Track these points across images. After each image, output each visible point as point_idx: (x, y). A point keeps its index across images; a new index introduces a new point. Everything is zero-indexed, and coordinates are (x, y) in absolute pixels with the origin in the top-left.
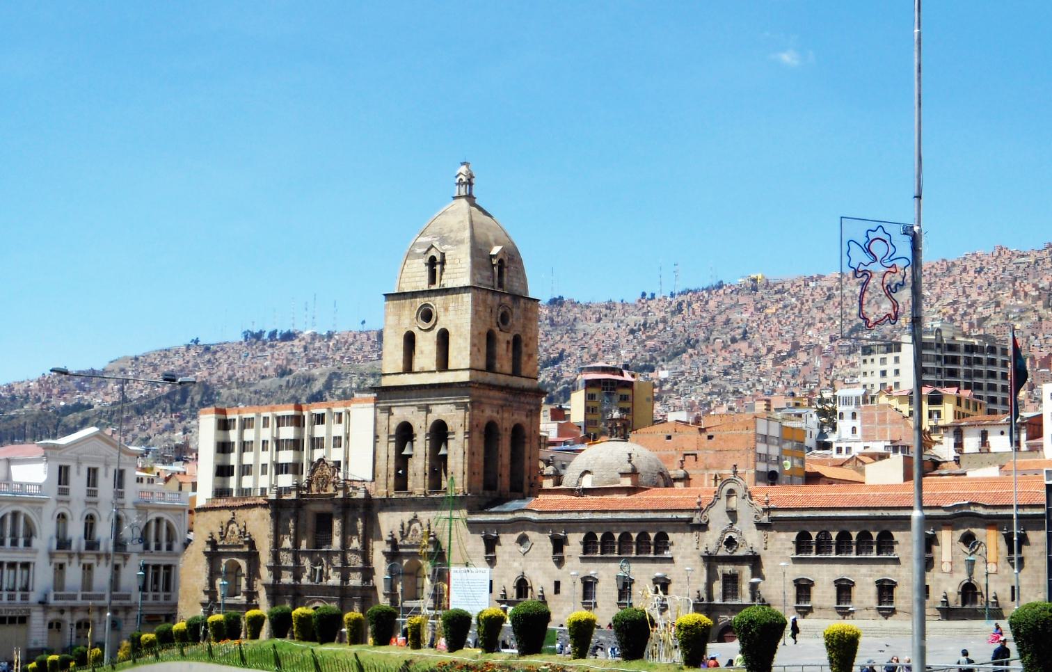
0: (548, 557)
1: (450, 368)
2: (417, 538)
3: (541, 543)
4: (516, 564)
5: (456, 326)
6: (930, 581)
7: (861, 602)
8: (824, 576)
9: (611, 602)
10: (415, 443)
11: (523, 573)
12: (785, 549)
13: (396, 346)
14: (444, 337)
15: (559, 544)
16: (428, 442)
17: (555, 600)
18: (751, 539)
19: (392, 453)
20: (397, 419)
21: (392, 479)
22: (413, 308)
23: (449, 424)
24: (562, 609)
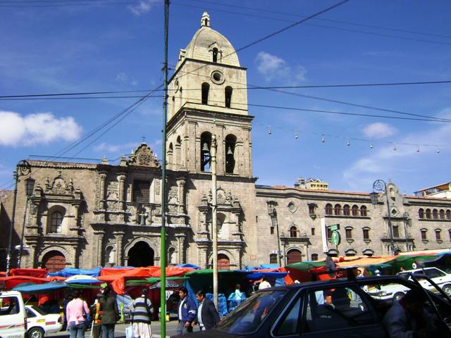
3: (302, 205)
4: (288, 218)
8: (431, 226)
14: (229, 92)
15: (312, 207)
23: (238, 137)
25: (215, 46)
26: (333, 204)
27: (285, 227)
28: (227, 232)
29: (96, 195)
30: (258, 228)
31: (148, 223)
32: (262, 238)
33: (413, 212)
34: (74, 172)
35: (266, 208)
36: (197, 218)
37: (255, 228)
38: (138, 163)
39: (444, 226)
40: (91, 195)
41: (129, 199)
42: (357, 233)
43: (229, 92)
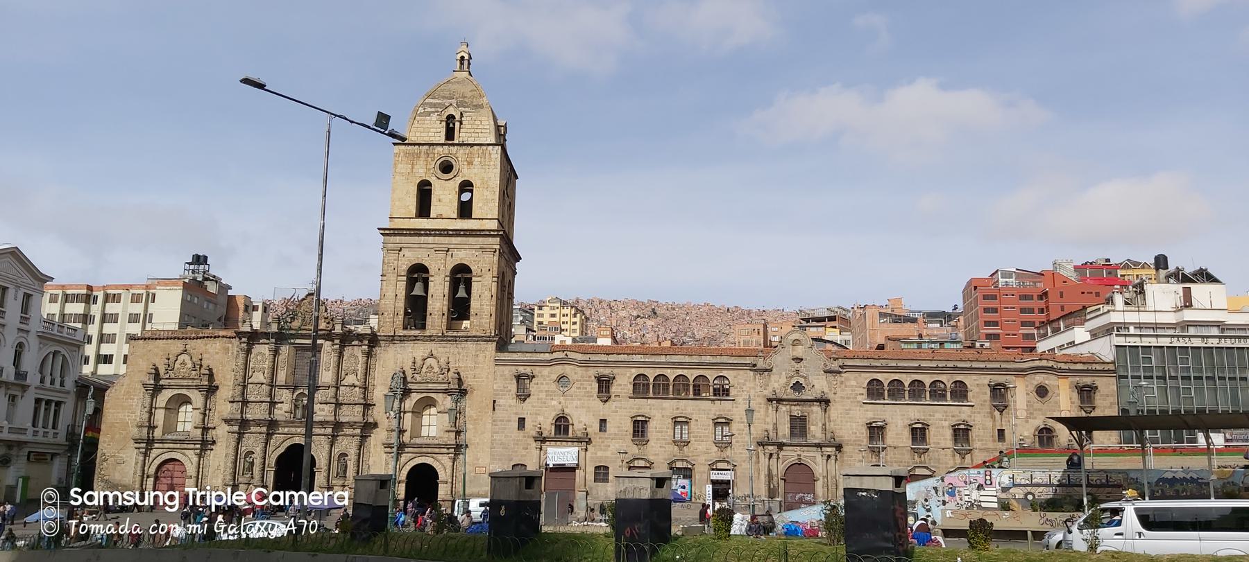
0: (592, 396)
1: (473, 217)
4: (554, 403)
6: (1006, 425)
7: (939, 443)
9: (664, 439)
10: (431, 284)
12: (857, 394)
15: (604, 384)
16: (447, 284)
17: (600, 438)
18: (819, 384)
19: (402, 293)
21: (401, 317)
22: (429, 159)
24: (609, 446)
26: (651, 374)
28: (433, 425)
32: (497, 437)
33: (857, 383)
35: (513, 386)
39: (938, 416)
40: (229, 377)
41: (282, 377)
43: (466, 186)
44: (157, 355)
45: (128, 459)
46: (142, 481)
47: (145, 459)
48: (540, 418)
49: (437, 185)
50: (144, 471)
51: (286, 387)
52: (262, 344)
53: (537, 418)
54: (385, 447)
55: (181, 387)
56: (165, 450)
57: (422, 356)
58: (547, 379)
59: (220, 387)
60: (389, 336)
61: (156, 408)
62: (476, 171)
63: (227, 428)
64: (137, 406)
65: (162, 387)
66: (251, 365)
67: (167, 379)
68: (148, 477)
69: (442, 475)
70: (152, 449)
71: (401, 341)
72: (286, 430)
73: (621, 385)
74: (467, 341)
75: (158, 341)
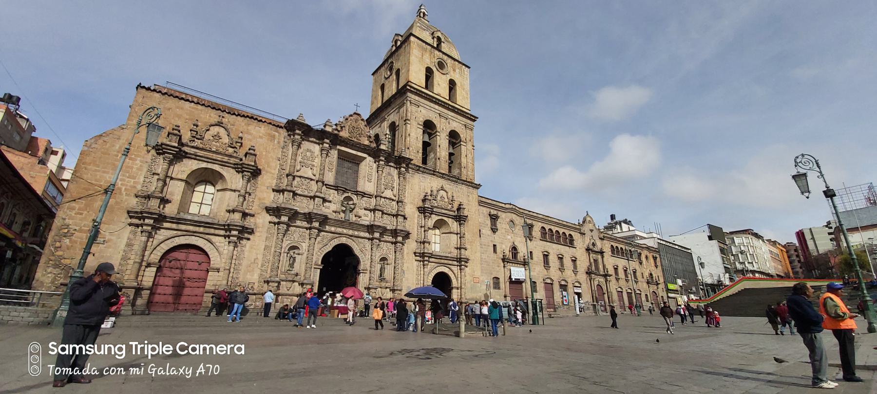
2: (441, 204)
4: (509, 237)
5: (461, 83)
11: (514, 243)
13: (420, 70)
20: (424, 116)
24: (535, 269)
25: (439, 34)
27: (506, 247)
29: (281, 165)
30: (481, 244)
31: (353, 218)
32: (484, 256)
34: (249, 125)
35: (489, 222)
36: (416, 221)
37: (478, 244)
38: (344, 134)
40: (273, 164)
41: (330, 178)
42: (568, 263)
43: (452, 84)
44: (179, 117)
45: (114, 238)
46: (139, 270)
47: (148, 241)
48: (504, 247)
49: (437, 76)
50: (143, 256)
51: (336, 188)
52: (312, 142)
53: (502, 246)
54: (416, 256)
55: (214, 161)
56: (179, 233)
57: (437, 188)
58: (505, 221)
59: (263, 172)
60: (417, 166)
61: (172, 178)
62: (457, 76)
63: (269, 218)
64: (138, 169)
65: (186, 156)
66: (299, 159)
67: (193, 147)
68: (149, 265)
69: (455, 283)
70: (159, 229)
71: (423, 172)
72: (333, 229)
73: (536, 231)
74: (463, 184)
75: (183, 101)
